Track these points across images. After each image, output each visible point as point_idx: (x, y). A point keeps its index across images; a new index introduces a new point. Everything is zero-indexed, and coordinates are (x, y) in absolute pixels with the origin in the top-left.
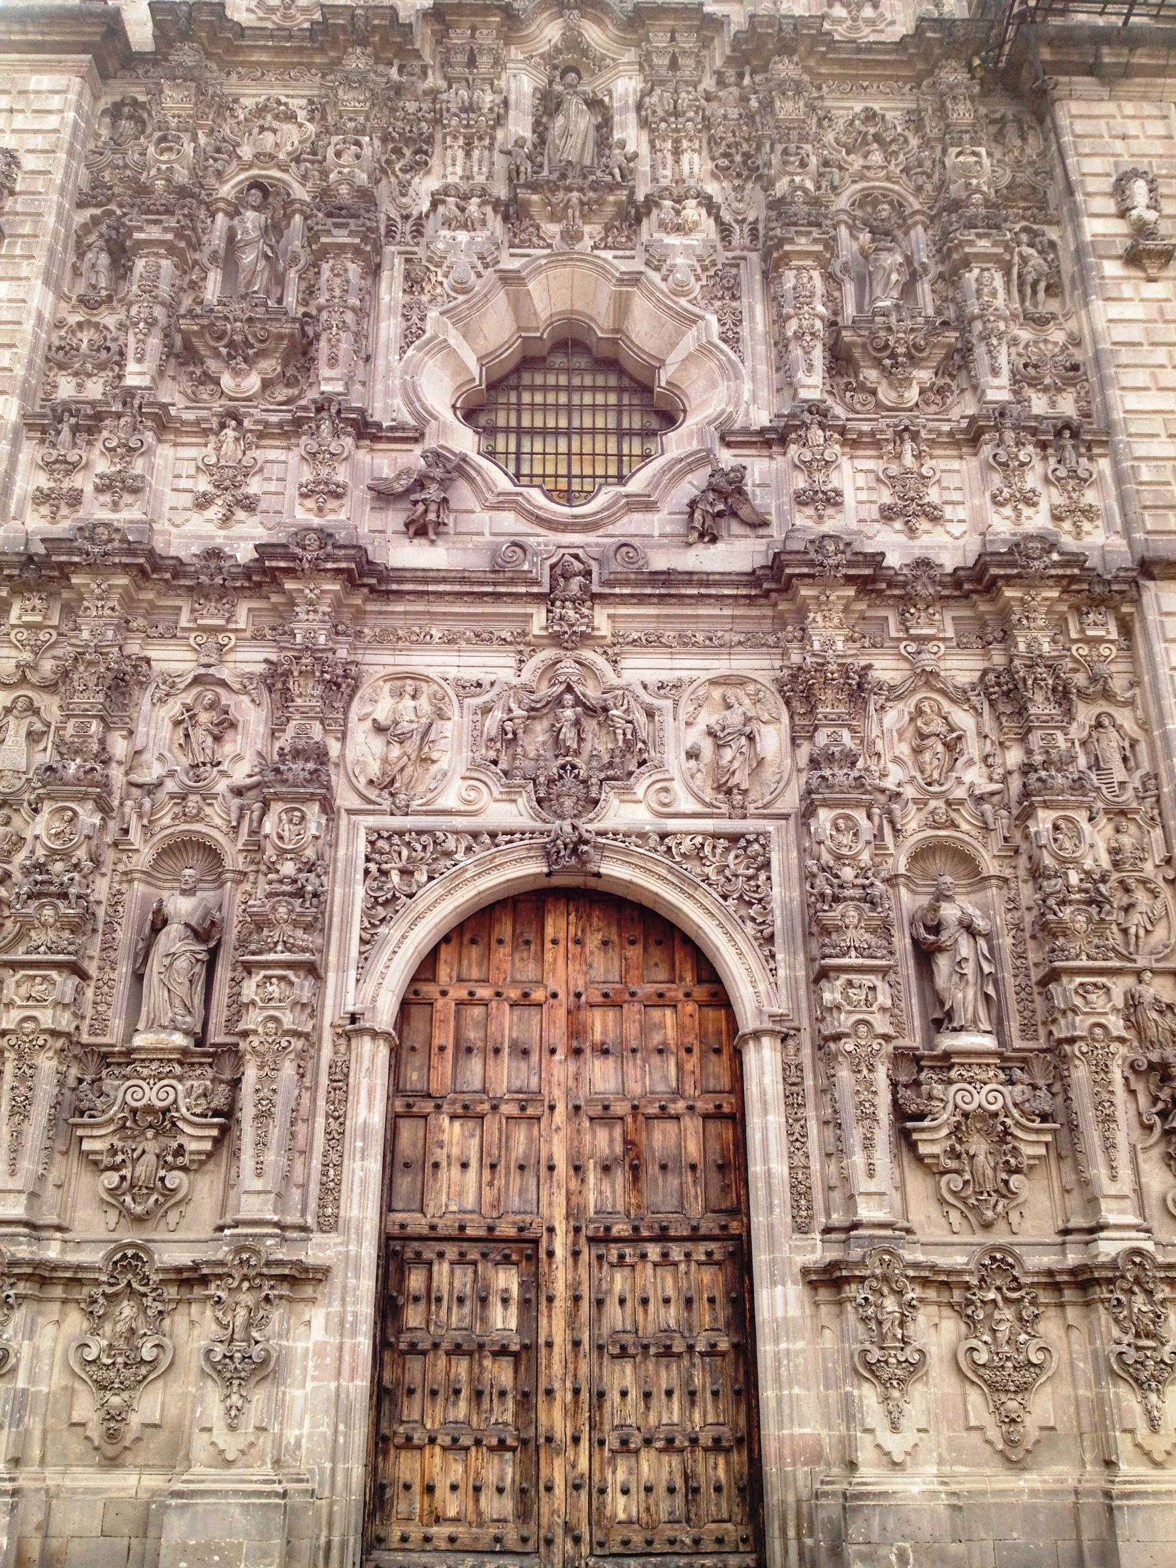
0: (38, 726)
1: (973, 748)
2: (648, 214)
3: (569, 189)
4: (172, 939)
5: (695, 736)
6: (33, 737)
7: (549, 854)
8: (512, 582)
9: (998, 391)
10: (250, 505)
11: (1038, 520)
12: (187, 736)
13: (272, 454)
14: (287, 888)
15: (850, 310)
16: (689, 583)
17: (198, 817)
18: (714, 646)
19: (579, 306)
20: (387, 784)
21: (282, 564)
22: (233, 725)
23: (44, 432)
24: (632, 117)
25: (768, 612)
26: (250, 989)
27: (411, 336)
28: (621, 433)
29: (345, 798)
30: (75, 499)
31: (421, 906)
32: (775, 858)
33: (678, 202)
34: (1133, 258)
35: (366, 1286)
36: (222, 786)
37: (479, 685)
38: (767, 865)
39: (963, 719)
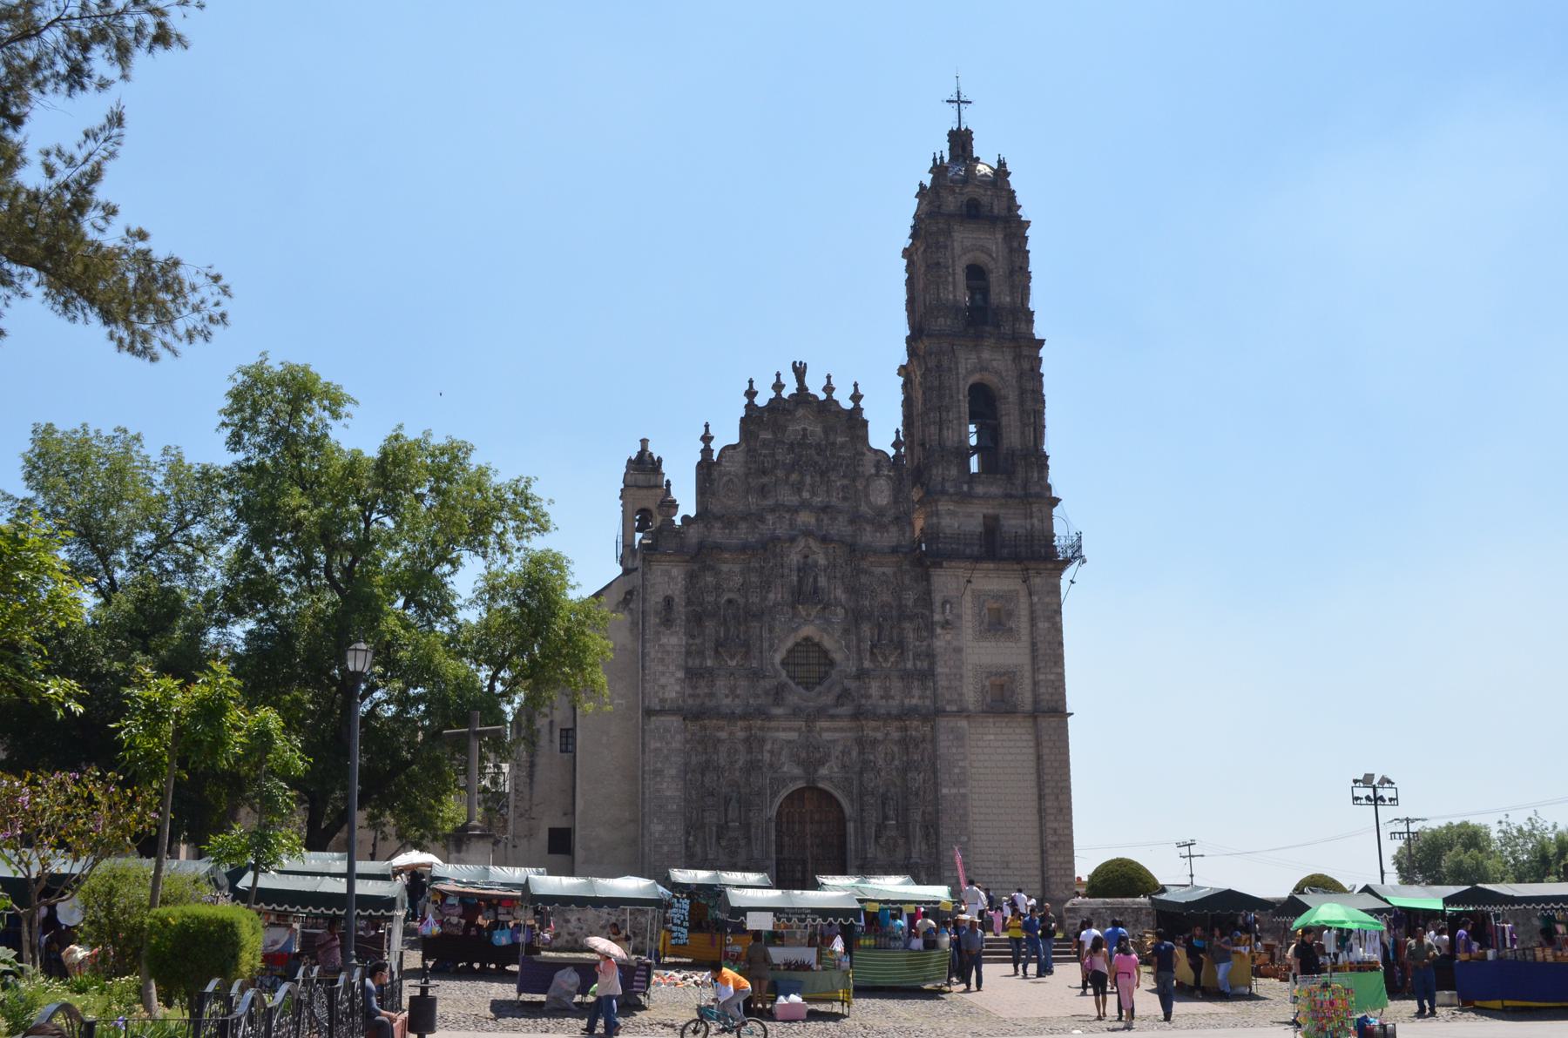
1: (897, 757)
4: (734, 803)
5: (837, 753)
9: (909, 665)
10: (738, 696)
11: (914, 701)
15: (876, 637)
18: (842, 730)
20: (771, 765)
24: (823, 574)
26: (751, 814)
27: (771, 646)
28: (819, 664)
29: (765, 770)
30: (698, 695)
35: (774, 869)
36: (737, 766)
39: (896, 749)
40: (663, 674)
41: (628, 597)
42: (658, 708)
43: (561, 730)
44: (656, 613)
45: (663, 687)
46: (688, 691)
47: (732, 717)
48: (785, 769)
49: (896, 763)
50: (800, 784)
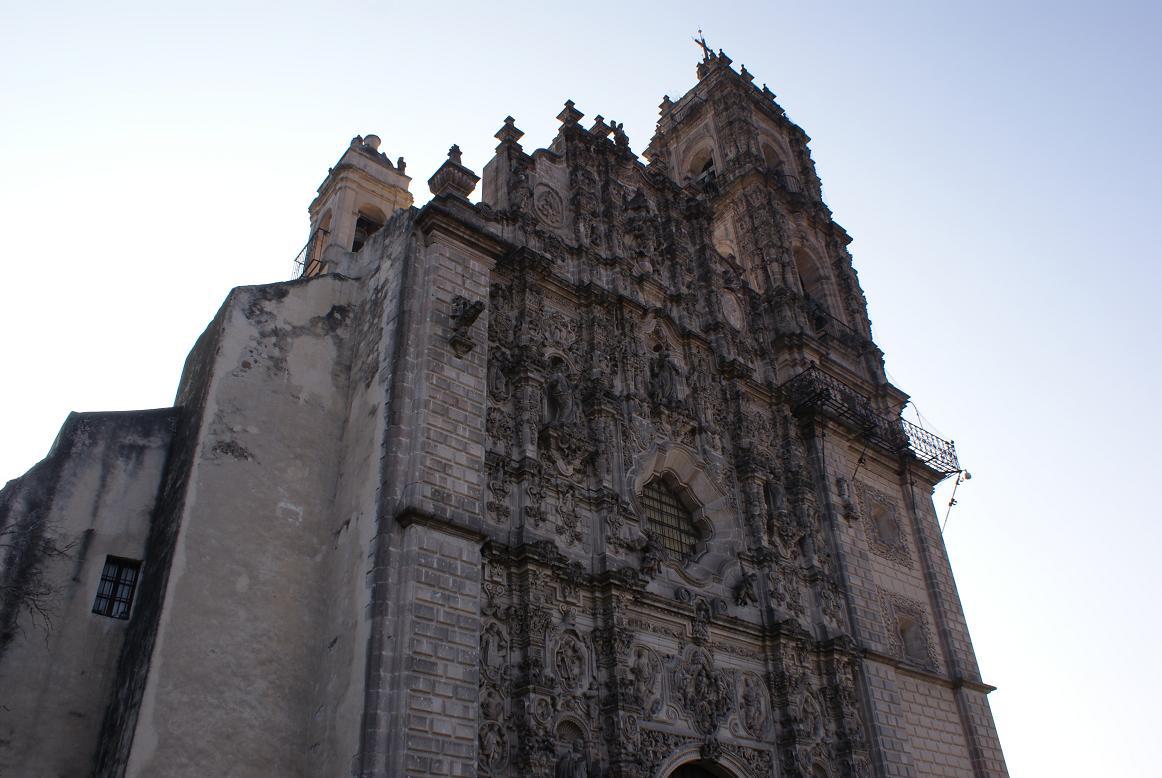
0: (503, 643)
2: (700, 434)
3: (679, 414)
6: (500, 648)
7: (702, 750)
8: (684, 609)
10: (578, 537)
12: (563, 660)
13: (585, 513)
14: (631, 759)
16: (742, 625)
17: (573, 709)
18: (742, 654)
19: (674, 468)
21: (617, 582)
22: (580, 659)
23: (490, 469)
25: (760, 643)
31: (663, 768)
32: (775, 763)
33: (713, 433)
34: (847, 517)
36: (579, 692)
37: (668, 657)
38: (771, 767)
40: (445, 441)
41: (337, 316)
42: (429, 507)
43: (111, 560)
44: (438, 321)
45: (444, 468)
46: (489, 497)
47: (568, 576)
48: (662, 715)
49: (822, 733)
50: (696, 756)
